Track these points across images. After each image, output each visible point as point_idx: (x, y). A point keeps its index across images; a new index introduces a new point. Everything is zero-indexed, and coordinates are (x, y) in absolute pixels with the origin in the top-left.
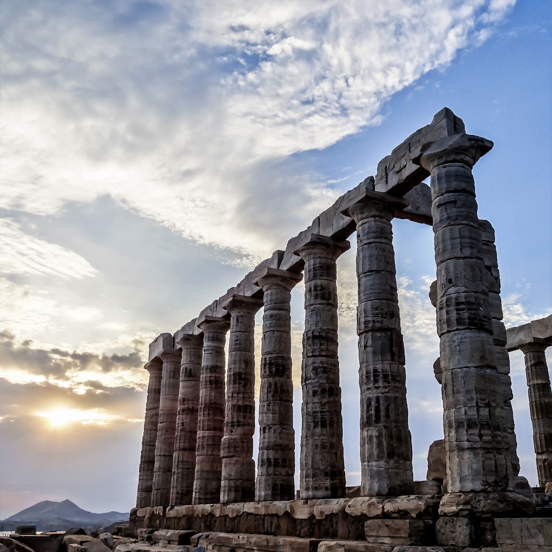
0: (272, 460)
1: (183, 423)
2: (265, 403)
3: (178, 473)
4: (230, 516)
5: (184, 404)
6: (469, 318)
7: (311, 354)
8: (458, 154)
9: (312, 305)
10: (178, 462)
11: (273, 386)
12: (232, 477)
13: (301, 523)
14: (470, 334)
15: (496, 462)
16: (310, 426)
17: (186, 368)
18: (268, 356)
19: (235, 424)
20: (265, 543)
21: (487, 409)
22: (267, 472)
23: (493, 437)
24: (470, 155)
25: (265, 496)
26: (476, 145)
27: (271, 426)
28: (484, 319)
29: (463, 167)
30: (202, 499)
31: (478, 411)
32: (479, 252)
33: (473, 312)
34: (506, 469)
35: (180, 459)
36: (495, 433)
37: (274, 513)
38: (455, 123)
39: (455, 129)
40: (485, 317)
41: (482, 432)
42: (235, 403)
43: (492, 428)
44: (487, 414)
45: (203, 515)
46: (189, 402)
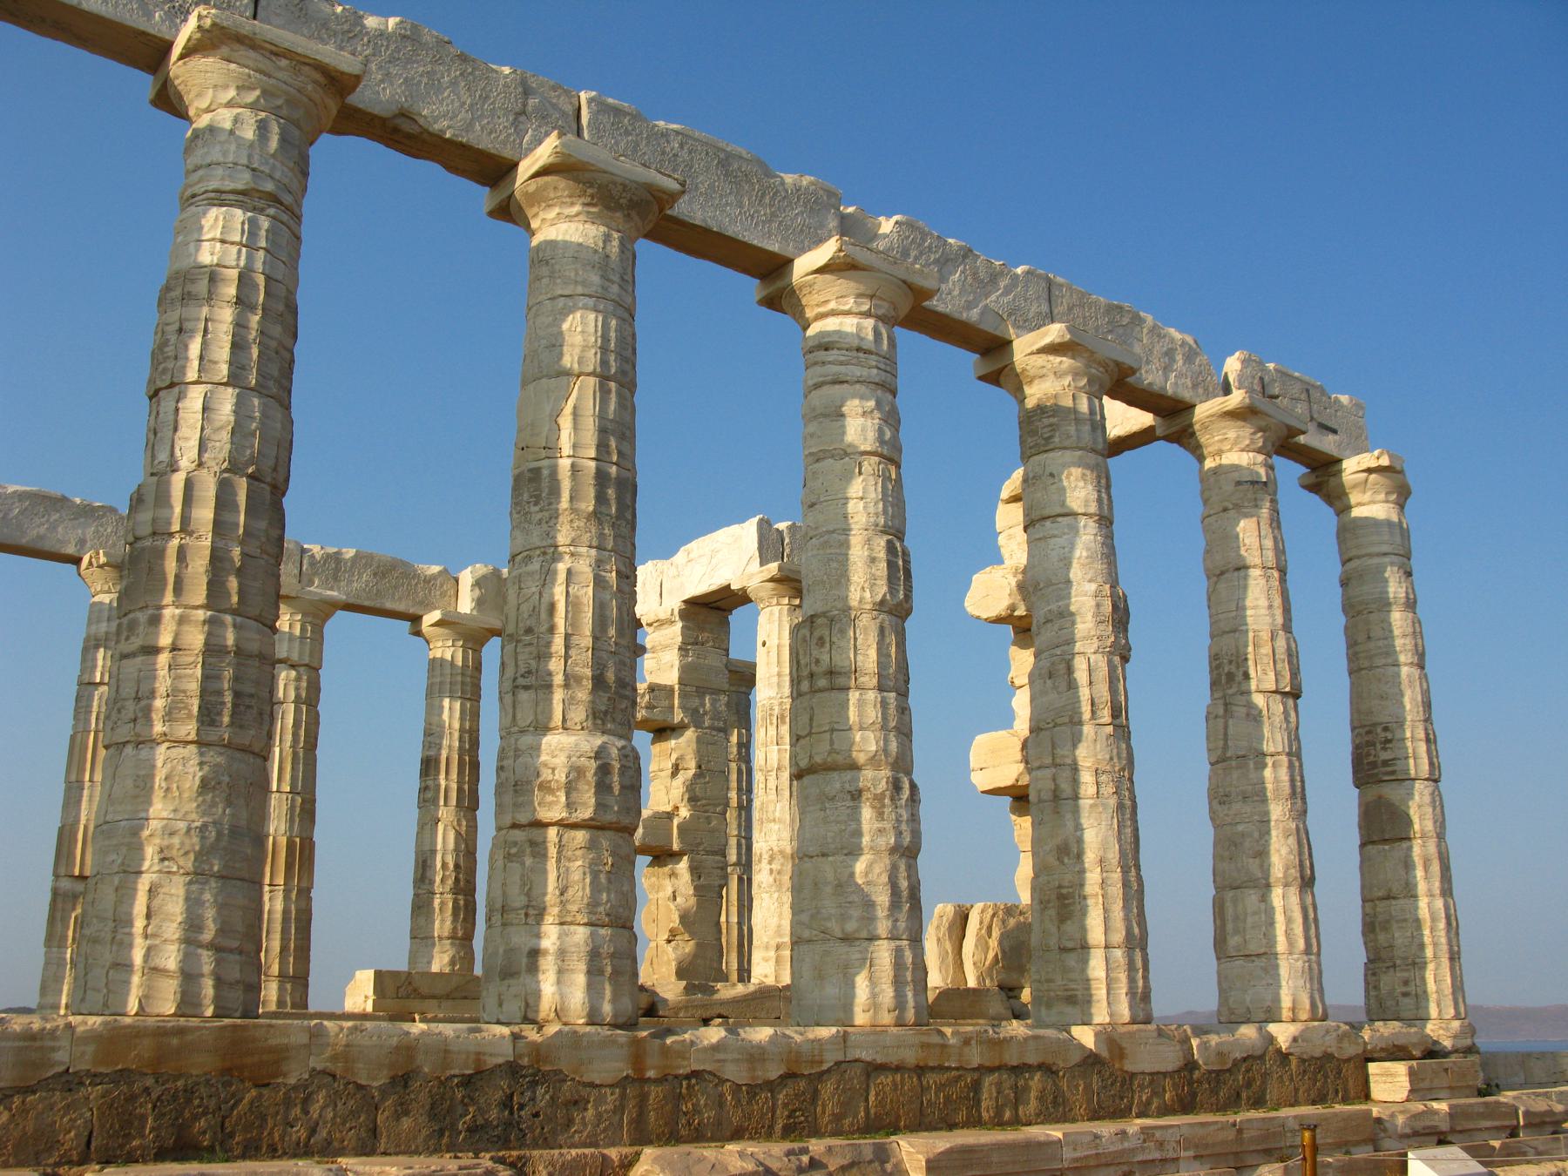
4: (735, 1073)
37: (1032, 1059)
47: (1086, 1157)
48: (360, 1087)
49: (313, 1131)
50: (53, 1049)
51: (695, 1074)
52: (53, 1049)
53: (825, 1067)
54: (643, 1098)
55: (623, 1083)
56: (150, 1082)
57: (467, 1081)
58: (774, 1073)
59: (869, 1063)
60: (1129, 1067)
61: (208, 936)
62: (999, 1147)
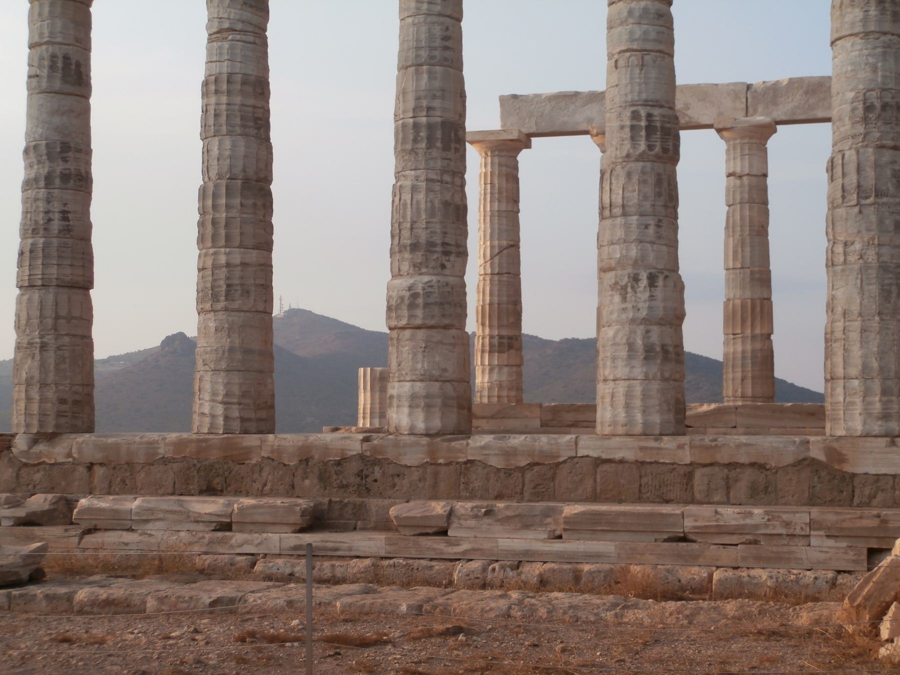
0: (671, 349)
1: (64, 212)
2: (652, 221)
3: (59, 348)
4: (496, 462)
5: (65, 160)
7: (890, 143)
9: (885, 34)
10: (57, 317)
11: (665, 185)
12: (448, 375)
13: (877, 481)
16: (890, 292)
17: (66, 58)
18: (656, 112)
19: (453, 249)
20: (875, 523)
22: (662, 375)
25: (662, 423)
27: (666, 273)
30: (249, 420)
35: (63, 312)
37: (743, 459)
42: (448, 197)
45: (307, 461)
46: (78, 155)
47: (706, 527)
48: (285, 465)
49: (265, 485)
50: (158, 448)
51: (469, 462)
52: (158, 448)
53: (561, 460)
54: (436, 475)
55: (423, 466)
56: (195, 462)
57: (338, 463)
58: (523, 463)
59: (597, 459)
60: (848, 468)
61: (220, 398)
62: (624, 514)
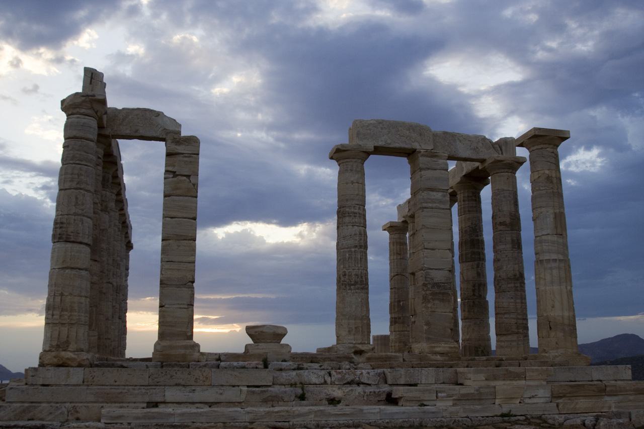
6: (60, 234)
8: (75, 108)
14: (58, 246)
15: (59, 332)
21: (60, 298)
23: (61, 316)
24: (84, 107)
26: (87, 100)
28: (70, 234)
29: (78, 118)
31: (54, 298)
32: (78, 184)
33: (64, 229)
34: (68, 337)
36: (62, 313)
38: (92, 78)
39: (91, 83)
40: (72, 232)
41: (55, 313)
43: (60, 310)
44: (59, 300)
